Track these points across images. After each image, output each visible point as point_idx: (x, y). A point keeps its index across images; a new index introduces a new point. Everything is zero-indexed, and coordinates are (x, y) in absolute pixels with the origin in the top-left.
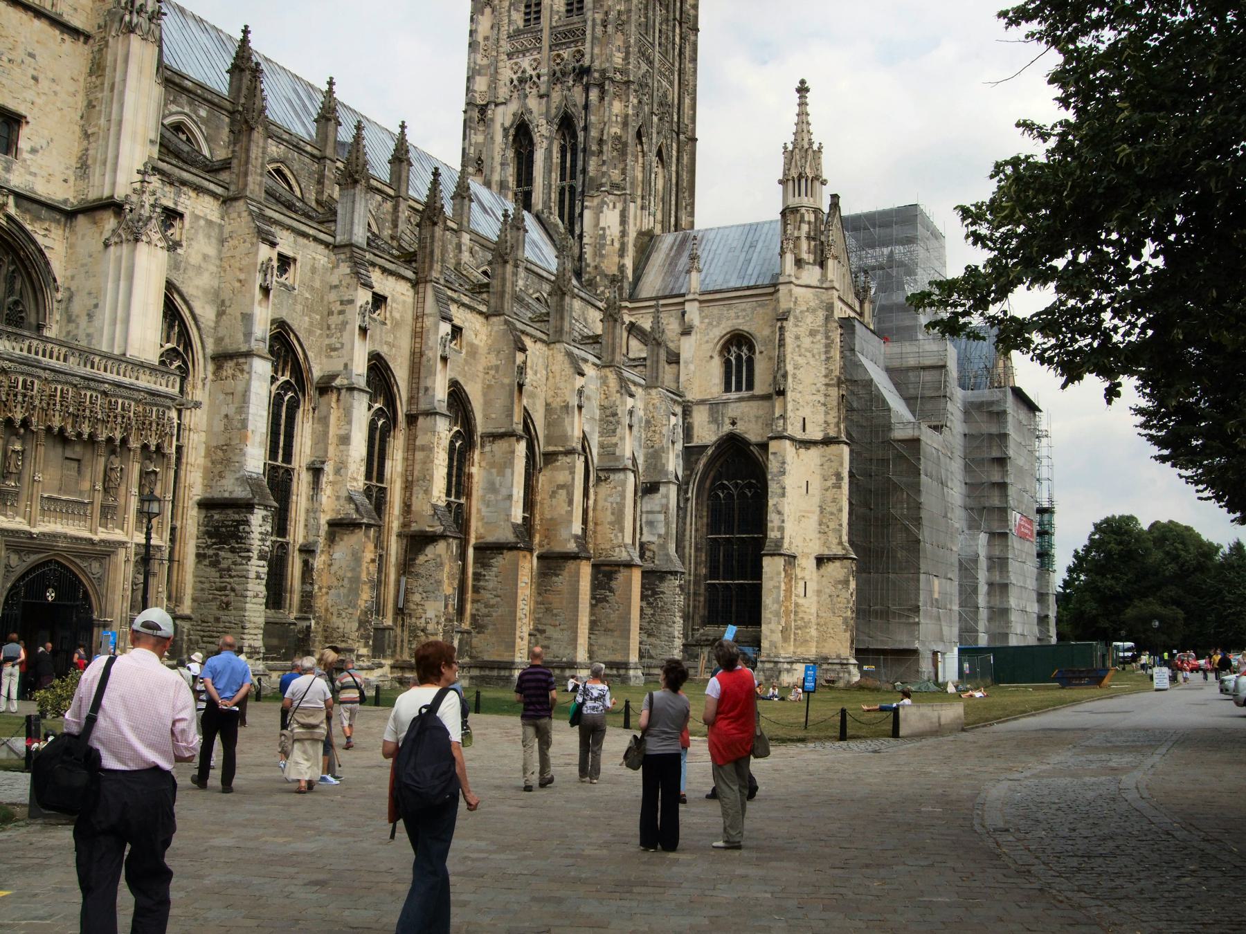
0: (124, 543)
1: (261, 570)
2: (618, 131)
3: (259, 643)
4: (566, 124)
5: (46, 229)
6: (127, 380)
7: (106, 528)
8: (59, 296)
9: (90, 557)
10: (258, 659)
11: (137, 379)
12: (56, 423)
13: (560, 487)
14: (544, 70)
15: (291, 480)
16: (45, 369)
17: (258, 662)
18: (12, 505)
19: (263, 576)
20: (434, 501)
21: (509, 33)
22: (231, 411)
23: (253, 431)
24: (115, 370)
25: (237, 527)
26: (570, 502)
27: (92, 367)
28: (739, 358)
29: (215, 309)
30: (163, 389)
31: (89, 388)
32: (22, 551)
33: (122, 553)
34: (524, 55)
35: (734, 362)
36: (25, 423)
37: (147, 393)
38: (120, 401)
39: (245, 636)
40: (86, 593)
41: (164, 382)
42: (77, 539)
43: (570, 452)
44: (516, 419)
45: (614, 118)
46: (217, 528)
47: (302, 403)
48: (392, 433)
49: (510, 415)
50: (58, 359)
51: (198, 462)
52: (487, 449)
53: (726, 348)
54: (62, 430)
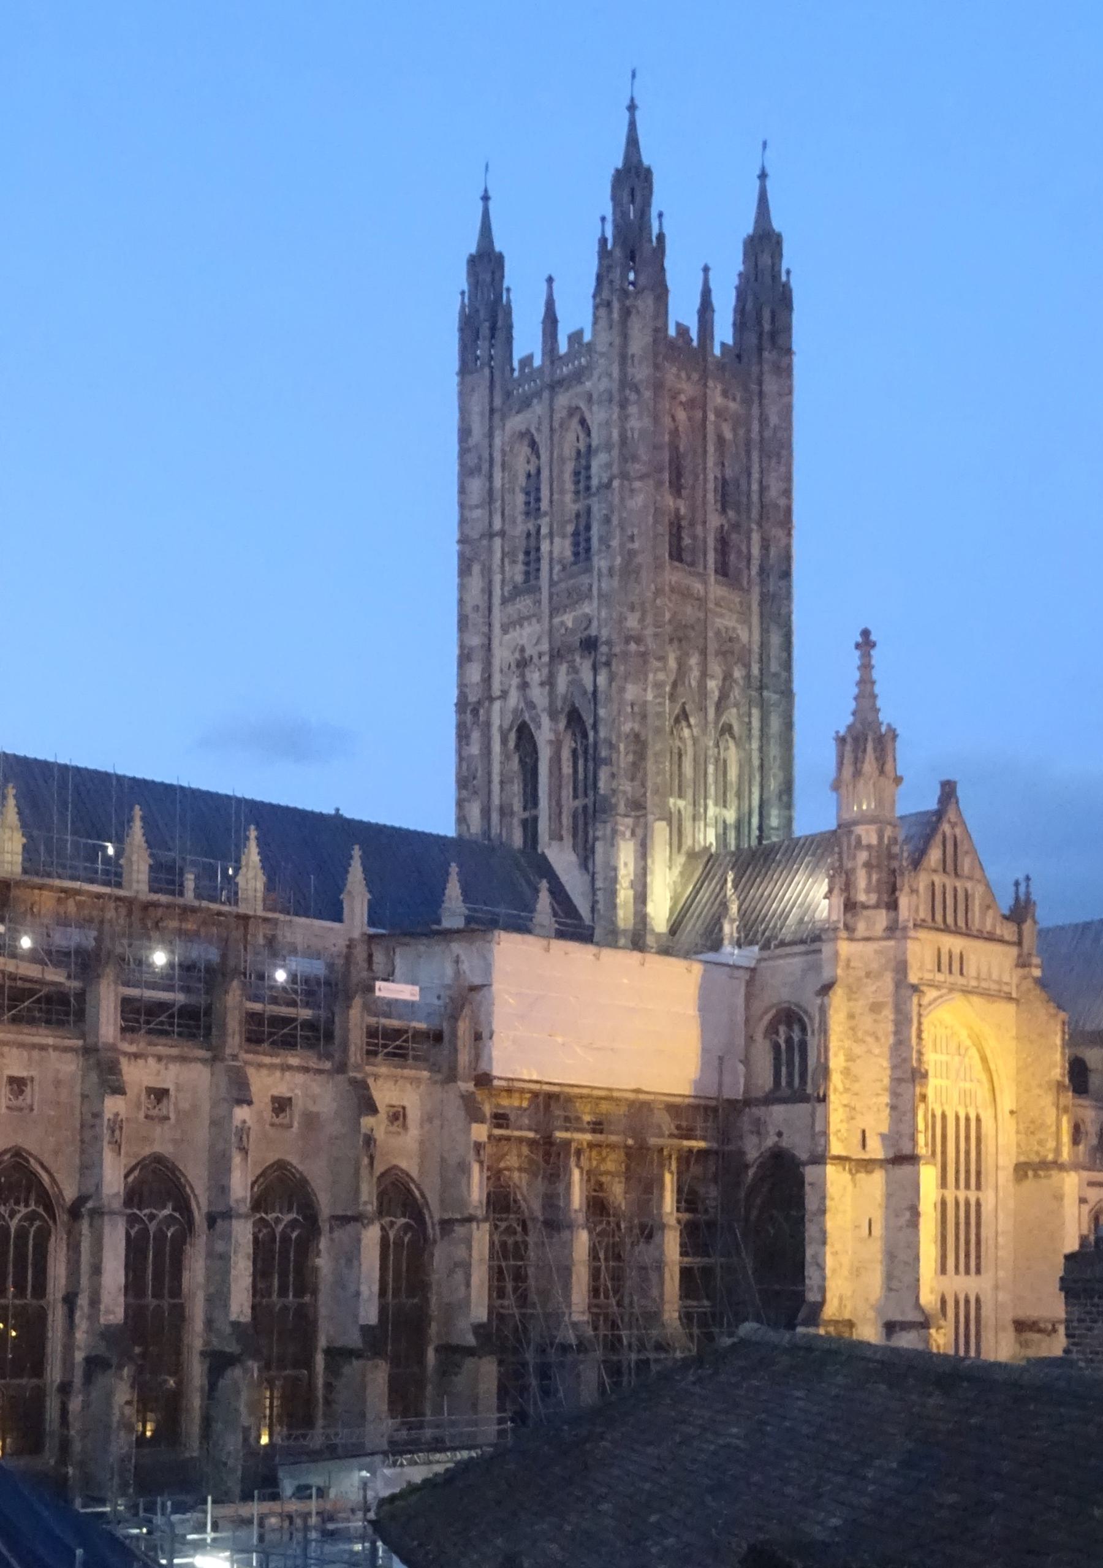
2: (637, 727)
4: (574, 718)
13: (456, 1265)
14: (545, 647)
20: (233, 1317)
21: (503, 595)
26: (468, 1285)
28: (789, 1040)
34: (521, 626)
35: (783, 1046)
43: (470, 1219)
44: (364, 1197)
45: (629, 709)
47: (53, 1230)
48: (188, 1240)
49: (357, 1191)
52: (336, 1235)
53: (772, 1030)
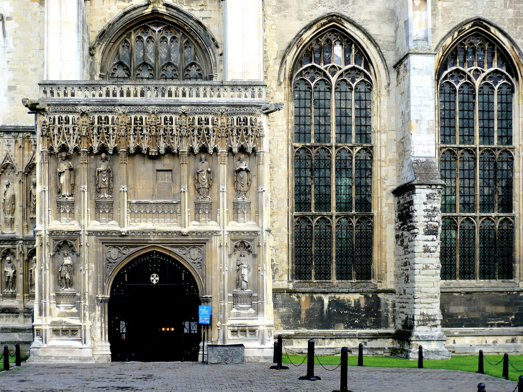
0: (216, 232)
1: (429, 244)
3: (435, 310)
5: (202, 5)
6: (206, 100)
7: (199, 221)
8: (219, 51)
9: (187, 247)
10: (436, 326)
11: (219, 96)
12: (132, 145)
15: (512, 159)
16: (121, 105)
17: (434, 329)
18: (104, 212)
19: (432, 249)
22: (403, 107)
23: (417, 121)
24: (194, 94)
25: (408, 208)
27: (170, 95)
29: (394, 26)
30: (249, 100)
31: (161, 112)
32: (121, 246)
33: (216, 241)
36: (103, 149)
37: (228, 106)
38: (196, 117)
39: (416, 306)
40: (190, 276)
41: (249, 94)
42: (167, 233)
46: (402, 211)
50: (136, 95)
51: (390, 156)
54: (138, 150)
